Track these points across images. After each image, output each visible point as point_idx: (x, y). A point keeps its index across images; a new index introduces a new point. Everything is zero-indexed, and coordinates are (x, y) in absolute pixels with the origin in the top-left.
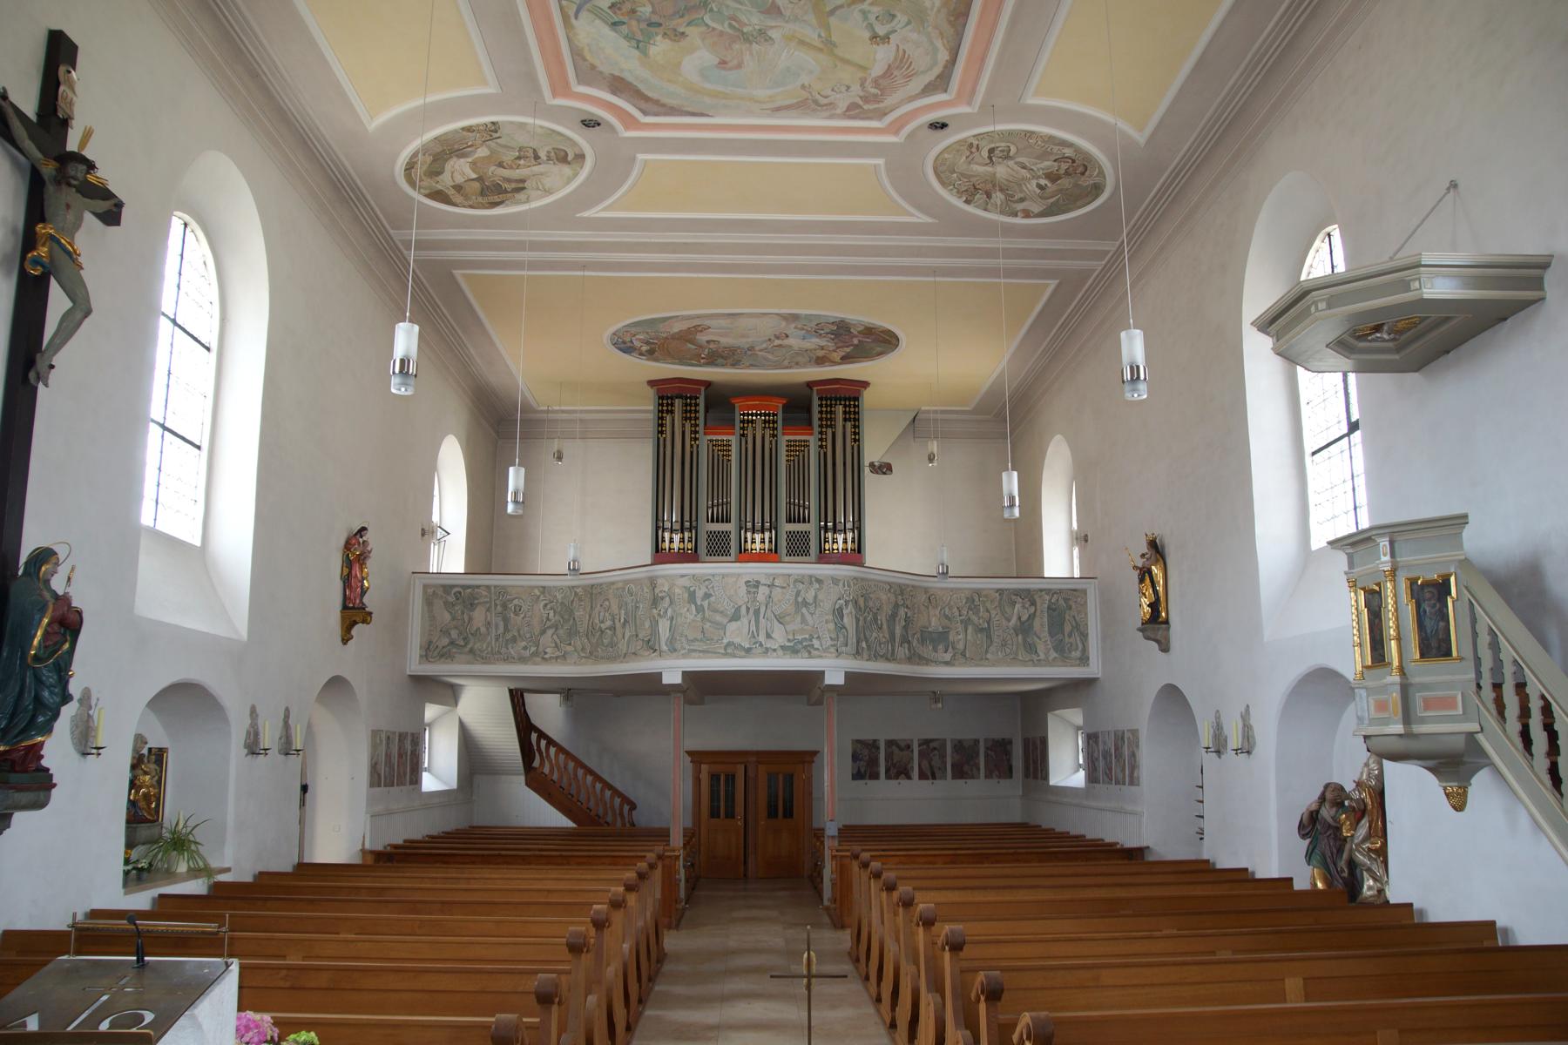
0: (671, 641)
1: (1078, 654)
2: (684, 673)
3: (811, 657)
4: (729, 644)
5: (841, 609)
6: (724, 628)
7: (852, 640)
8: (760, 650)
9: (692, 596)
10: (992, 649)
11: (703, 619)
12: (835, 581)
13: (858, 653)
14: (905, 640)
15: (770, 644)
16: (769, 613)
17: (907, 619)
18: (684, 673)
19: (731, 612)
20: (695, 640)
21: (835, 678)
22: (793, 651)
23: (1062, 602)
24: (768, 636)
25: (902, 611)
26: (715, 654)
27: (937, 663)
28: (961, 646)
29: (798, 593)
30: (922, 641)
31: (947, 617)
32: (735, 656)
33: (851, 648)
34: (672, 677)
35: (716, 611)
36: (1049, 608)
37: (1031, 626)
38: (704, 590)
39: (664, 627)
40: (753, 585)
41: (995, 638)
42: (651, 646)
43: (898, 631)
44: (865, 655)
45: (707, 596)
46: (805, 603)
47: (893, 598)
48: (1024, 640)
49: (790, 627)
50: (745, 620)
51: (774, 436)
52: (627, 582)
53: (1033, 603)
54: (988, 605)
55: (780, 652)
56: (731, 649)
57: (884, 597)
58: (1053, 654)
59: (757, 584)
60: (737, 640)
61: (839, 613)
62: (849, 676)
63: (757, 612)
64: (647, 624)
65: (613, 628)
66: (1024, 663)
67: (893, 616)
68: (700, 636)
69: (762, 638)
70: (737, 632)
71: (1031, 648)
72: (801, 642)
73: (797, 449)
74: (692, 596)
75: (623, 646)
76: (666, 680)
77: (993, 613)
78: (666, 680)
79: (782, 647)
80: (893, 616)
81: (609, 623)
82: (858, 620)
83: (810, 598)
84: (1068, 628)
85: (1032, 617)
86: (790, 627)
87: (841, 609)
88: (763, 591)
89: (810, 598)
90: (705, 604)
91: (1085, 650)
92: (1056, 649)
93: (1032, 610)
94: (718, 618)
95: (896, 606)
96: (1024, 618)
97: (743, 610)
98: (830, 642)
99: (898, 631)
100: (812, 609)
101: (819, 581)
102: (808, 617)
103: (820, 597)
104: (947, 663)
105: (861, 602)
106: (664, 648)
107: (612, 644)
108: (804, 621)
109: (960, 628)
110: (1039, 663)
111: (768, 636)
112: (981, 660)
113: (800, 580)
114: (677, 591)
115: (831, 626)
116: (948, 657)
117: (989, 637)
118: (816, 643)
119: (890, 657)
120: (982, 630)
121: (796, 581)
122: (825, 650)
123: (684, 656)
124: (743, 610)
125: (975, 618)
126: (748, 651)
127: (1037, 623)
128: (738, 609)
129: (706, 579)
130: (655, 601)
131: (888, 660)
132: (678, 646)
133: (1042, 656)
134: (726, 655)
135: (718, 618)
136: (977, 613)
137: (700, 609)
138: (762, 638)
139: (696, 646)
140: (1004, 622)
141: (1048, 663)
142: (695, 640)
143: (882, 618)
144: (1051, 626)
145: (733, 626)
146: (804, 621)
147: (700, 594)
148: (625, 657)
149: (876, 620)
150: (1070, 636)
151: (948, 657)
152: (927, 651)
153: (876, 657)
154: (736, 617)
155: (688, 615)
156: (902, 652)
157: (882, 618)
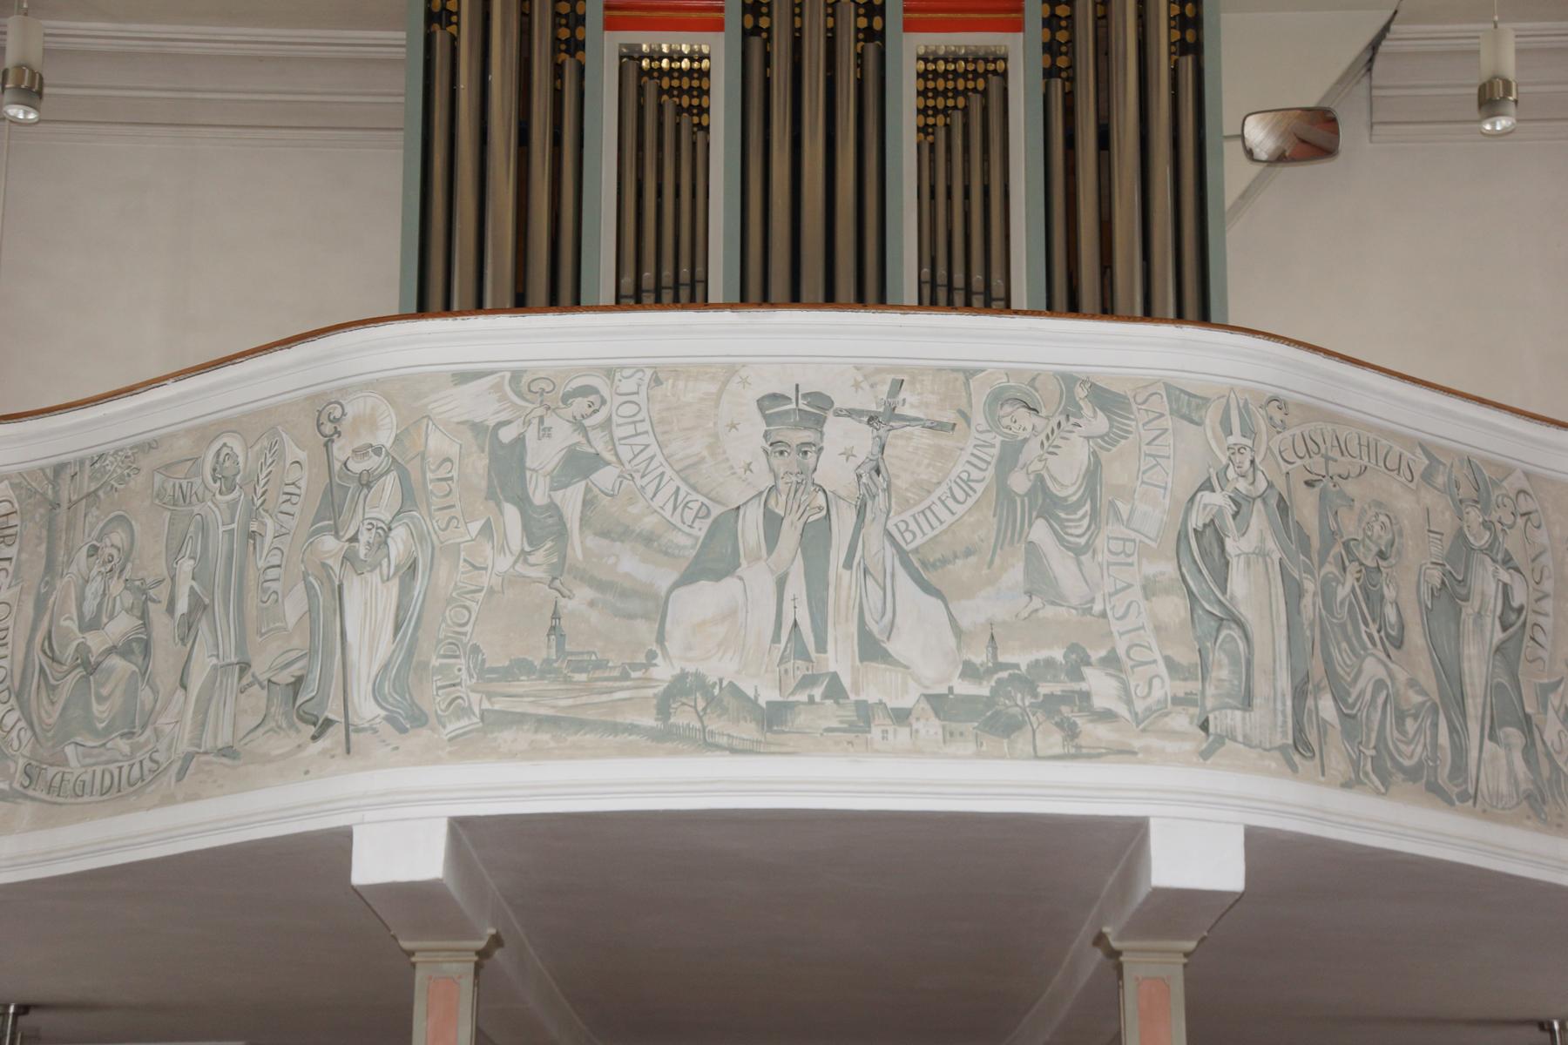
0: (404, 672)
2: (461, 828)
3: (1077, 753)
4: (681, 688)
5: (1213, 535)
6: (658, 611)
7: (1275, 683)
8: (832, 715)
9: (507, 469)
11: (559, 570)
12: (1186, 404)
13: (1301, 745)
14: (1511, 715)
15: (877, 687)
16: (873, 534)
17: (1510, 615)
18: (461, 828)
19: (689, 538)
20: (522, 667)
21: (1197, 855)
22: (989, 718)
24: (871, 649)
25: (1487, 580)
26: (612, 732)
29: (1010, 455)
32: (705, 743)
33: (1269, 716)
34: (399, 848)
35: (618, 532)
38: (563, 436)
39: (368, 610)
40: (799, 414)
42: (306, 709)
43: (1476, 668)
44: (1338, 762)
45: (579, 464)
46: (1045, 502)
47: (1445, 519)
49: (974, 612)
50: (757, 578)
51: (874, 36)
52: (206, 433)
55: (930, 727)
56: (692, 711)
57: (1406, 504)
59: (817, 410)
60: (721, 668)
61: (1205, 549)
62: (1263, 848)
63: (816, 538)
64: (293, 608)
65: (139, 647)
67: (1450, 594)
68: (540, 650)
69: (839, 658)
70: (722, 630)
72: (1027, 683)
73: (963, 94)
74: (507, 469)
75: (176, 725)
76: (371, 867)
78: (371, 867)
79: (940, 704)
80: (1450, 594)
81: (120, 626)
82: (1294, 593)
83: (1067, 469)
86: (974, 612)
87: (1213, 535)
88: (845, 443)
89: (1067, 469)
90: (571, 500)
94: (629, 564)
95: (1461, 549)
97: (751, 527)
98: (1165, 687)
99: (1476, 668)
100: (1078, 528)
101: (1107, 400)
102: (1061, 565)
103: (1116, 473)
105: (1306, 508)
106: (367, 709)
107: (132, 723)
108: (1039, 582)
111: (871, 649)
113: (1017, 396)
114: (437, 443)
115: (1173, 608)
118: (1101, 687)
119: (1450, 786)
121: (999, 398)
122: (1148, 721)
123: (464, 748)
124: (751, 527)
126: (773, 717)
128: (725, 525)
129: (576, 394)
130: (335, 500)
131: (1434, 789)
132: (432, 699)
134: (666, 738)
135: (629, 564)
137: (545, 527)
138: (839, 658)
139: (526, 695)
142: (522, 667)
143: (1404, 594)
145: (706, 598)
146: (1039, 582)
147: (544, 455)
148: (188, 772)
149: (1371, 595)
153: (1380, 771)
154: (715, 559)
155: (495, 550)
156: (1499, 763)
157: (1404, 594)
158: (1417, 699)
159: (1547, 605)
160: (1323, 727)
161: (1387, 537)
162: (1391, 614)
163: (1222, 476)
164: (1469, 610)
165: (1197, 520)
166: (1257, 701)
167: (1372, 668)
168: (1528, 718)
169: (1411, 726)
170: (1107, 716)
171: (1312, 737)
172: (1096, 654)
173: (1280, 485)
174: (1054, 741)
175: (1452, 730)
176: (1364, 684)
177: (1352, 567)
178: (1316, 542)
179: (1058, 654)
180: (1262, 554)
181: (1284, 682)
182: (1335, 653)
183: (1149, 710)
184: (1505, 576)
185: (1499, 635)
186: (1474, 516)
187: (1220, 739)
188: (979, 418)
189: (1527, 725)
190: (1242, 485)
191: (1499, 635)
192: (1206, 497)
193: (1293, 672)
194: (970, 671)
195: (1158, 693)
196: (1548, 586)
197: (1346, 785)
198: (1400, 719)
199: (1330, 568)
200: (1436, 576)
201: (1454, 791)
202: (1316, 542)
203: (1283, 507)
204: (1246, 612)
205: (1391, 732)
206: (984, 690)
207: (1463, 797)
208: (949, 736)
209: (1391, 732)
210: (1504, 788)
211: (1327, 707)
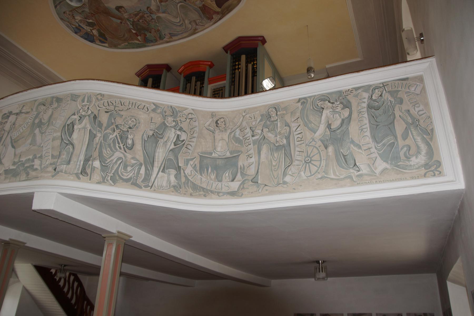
1: (421, 159)
5: (73, 124)
10: (293, 169)
16: (9, 136)
23: (386, 96)
25: (171, 135)
27: (218, 194)
28: (252, 171)
30: (202, 169)
31: (237, 140)
36: (370, 107)
37: (346, 133)
41: (297, 156)
44: (97, 176)
48: (337, 152)
53: (347, 105)
54: (288, 118)
58: (381, 165)
66: (338, 182)
71: (347, 161)
77: (294, 126)
84: (399, 127)
85: (346, 121)
91: (431, 152)
92: (385, 158)
93: (346, 113)
96: (336, 124)
104: (233, 194)
109: (252, 149)
110: (360, 180)
112: (280, 185)
116: (235, 185)
117: (289, 156)
120: (279, 148)
125: (270, 136)
127: (353, 128)
131: (135, 185)
133: (364, 169)
136: (273, 129)
140: (309, 135)
141: (373, 177)
144: (375, 126)
149: (123, 137)
150: (405, 137)
151: (235, 185)
152: (206, 180)
157: (136, 138)
158: (133, 162)
159: (194, 140)
160: (93, 169)
161: (133, 124)
162: (130, 142)
163: (78, 112)
164: (161, 142)
165: (69, 122)
166: (72, 162)
167: (118, 154)
168: (179, 167)
169: (129, 169)
170: (36, 169)
171: (88, 171)
172: (38, 156)
173: (96, 112)
174: (24, 176)
175: (146, 169)
176: (114, 158)
177: (117, 132)
178: (105, 125)
179: (31, 157)
180: (85, 128)
181: (82, 157)
182: (104, 151)
183: (44, 167)
184: (179, 133)
185: (172, 146)
186: (170, 119)
187: (58, 172)
188: (34, 110)
189: (178, 169)
190: (83, 113)
191: (172, 146)
192: (73, 117)
193: (86, 155)
194: (14, 164)
195: (47, 163)
196: (195, 135)
197: (99, 183)
198: (125, 167)
199: (109, 131)
200: (151, 133)
201: (142, 185)
202: (105, 125)
203: (95, 117)
204: (75, 142)
205: (121, 169)
206: (14, 167)
207: (146, 187)
208: (6, 178)
209: (121, 169)
210: (164, 184)
211: (97, 164)
